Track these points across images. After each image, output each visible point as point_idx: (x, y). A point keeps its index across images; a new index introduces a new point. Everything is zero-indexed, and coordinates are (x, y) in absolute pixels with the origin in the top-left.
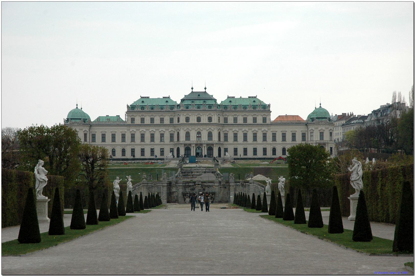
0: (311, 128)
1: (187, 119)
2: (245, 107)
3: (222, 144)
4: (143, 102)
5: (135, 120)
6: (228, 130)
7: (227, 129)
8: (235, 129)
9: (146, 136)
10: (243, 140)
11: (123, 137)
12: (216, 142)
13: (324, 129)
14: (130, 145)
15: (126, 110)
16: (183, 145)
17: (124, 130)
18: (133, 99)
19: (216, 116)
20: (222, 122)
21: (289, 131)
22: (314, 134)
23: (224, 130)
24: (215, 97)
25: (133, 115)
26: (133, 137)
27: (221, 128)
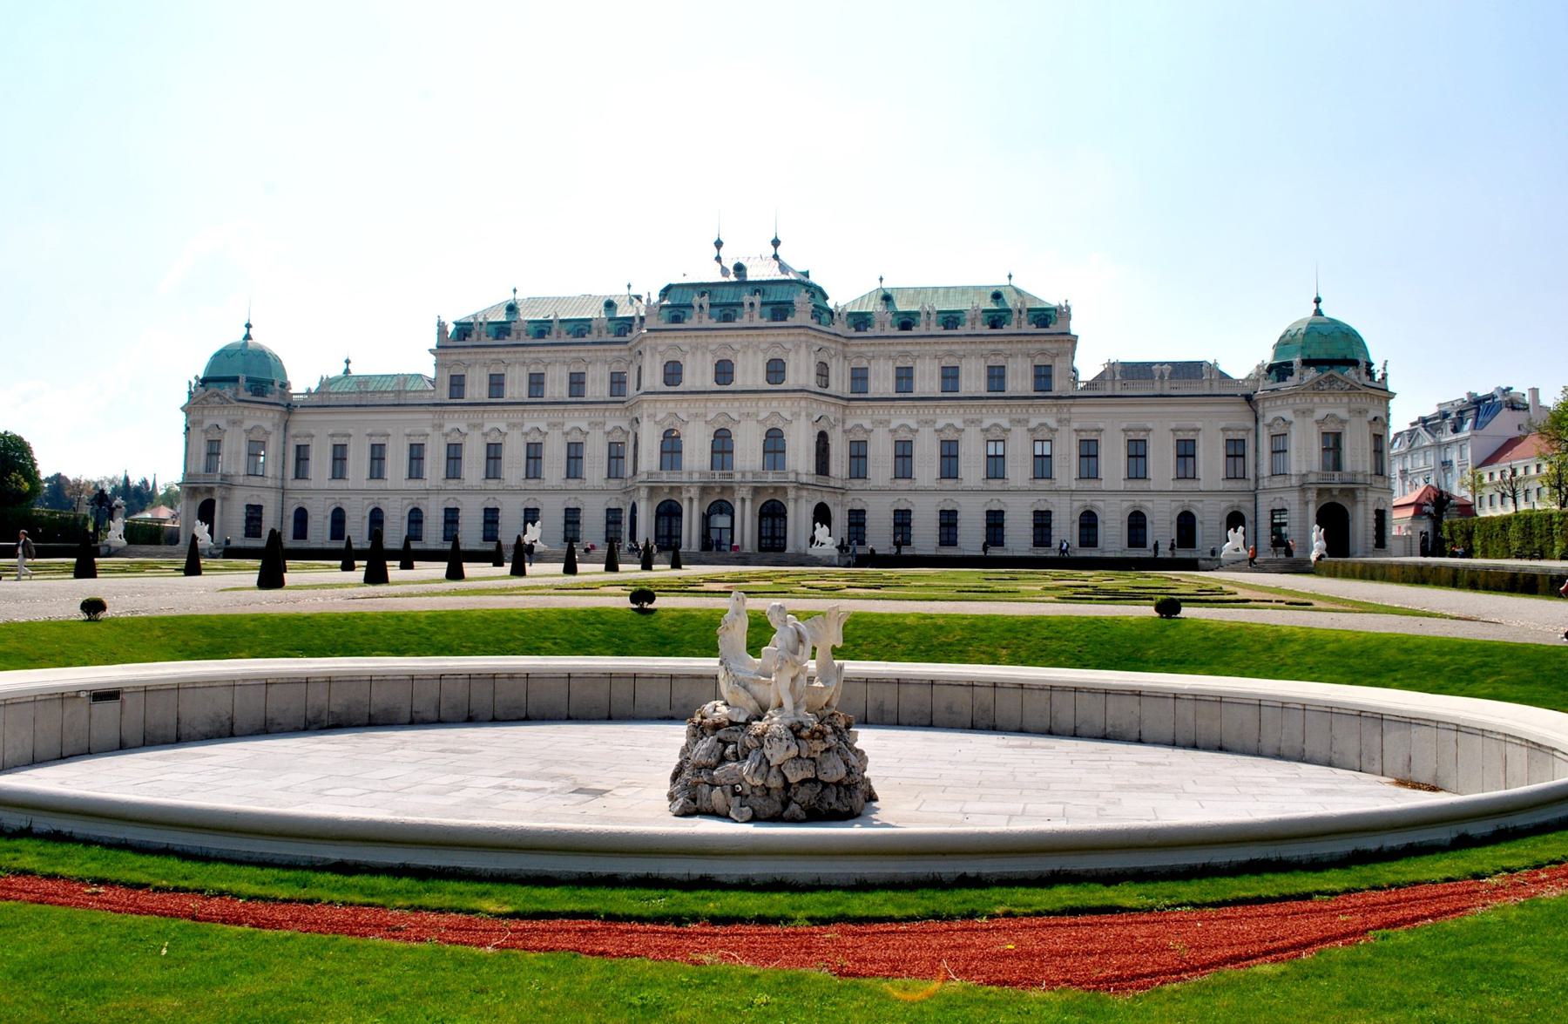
1: (673, 373)
2: (951, 320)
3: (843, 491)
4: (512, 309)
6: (867, 425)
7: (862, 418)
8: (903, 418)
9: (506, 454)
10: (936, 473)
11: (416, 455)
12: (804, 479)
13: (1342, 413)
14: (439, 491)
15: (433, 342)
16: (644, 493)
18: (478, 300)
19: (803, 351)
20: (840, 383)
22: (1293, 444)
23: (849, 425)
24: (813, 279)
25: (457, 363)
26: (454, 455)
27: (832, 412)
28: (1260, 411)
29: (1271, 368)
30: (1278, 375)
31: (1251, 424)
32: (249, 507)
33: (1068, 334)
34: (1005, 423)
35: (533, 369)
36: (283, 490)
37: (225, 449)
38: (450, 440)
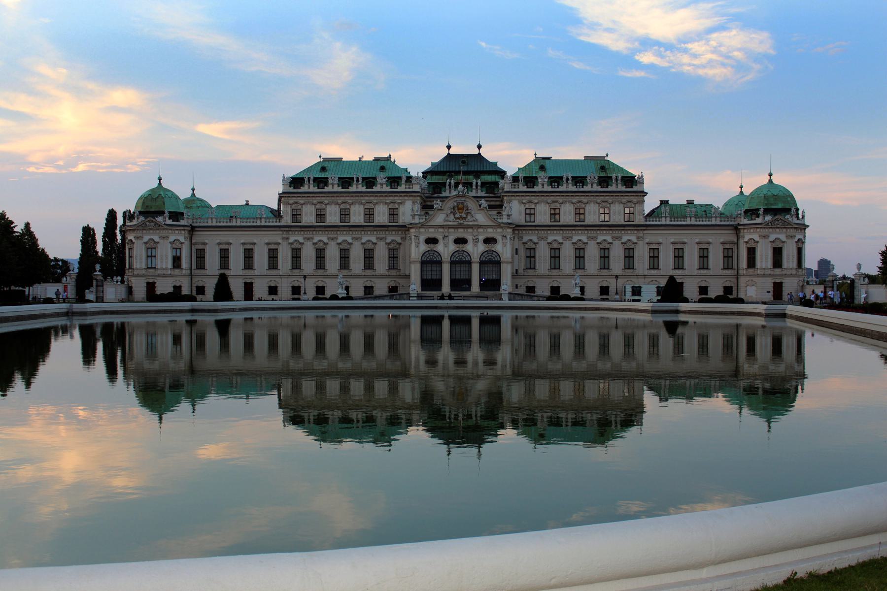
0: (747, 235)
2: (579, 180)
4: (323, 169)
5: (303, 214)
6: (535, 240)
8: (555, 237)
11: (273, 256)
13: (783, 237)
17: (276, 237)
21: (691, 242)
28: (742, 234)
29: (746, 212)
30: (751, 214)
31: (735, 240)
32: (175, 287)
33: (643, 192)
34: (610, 240)
35: (342, 207)
36: (191, 276)
37: (159, 252)
38: (293, 246)
